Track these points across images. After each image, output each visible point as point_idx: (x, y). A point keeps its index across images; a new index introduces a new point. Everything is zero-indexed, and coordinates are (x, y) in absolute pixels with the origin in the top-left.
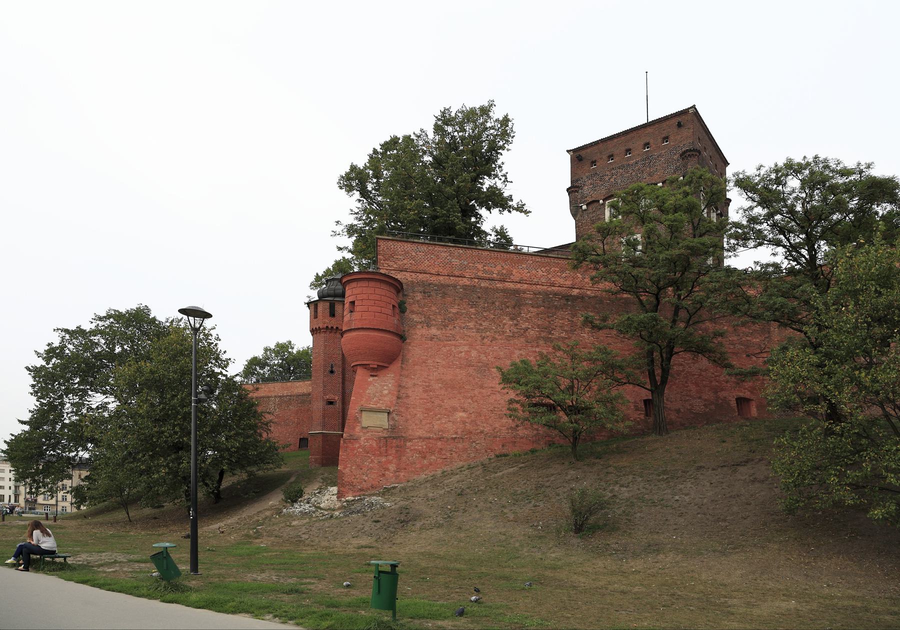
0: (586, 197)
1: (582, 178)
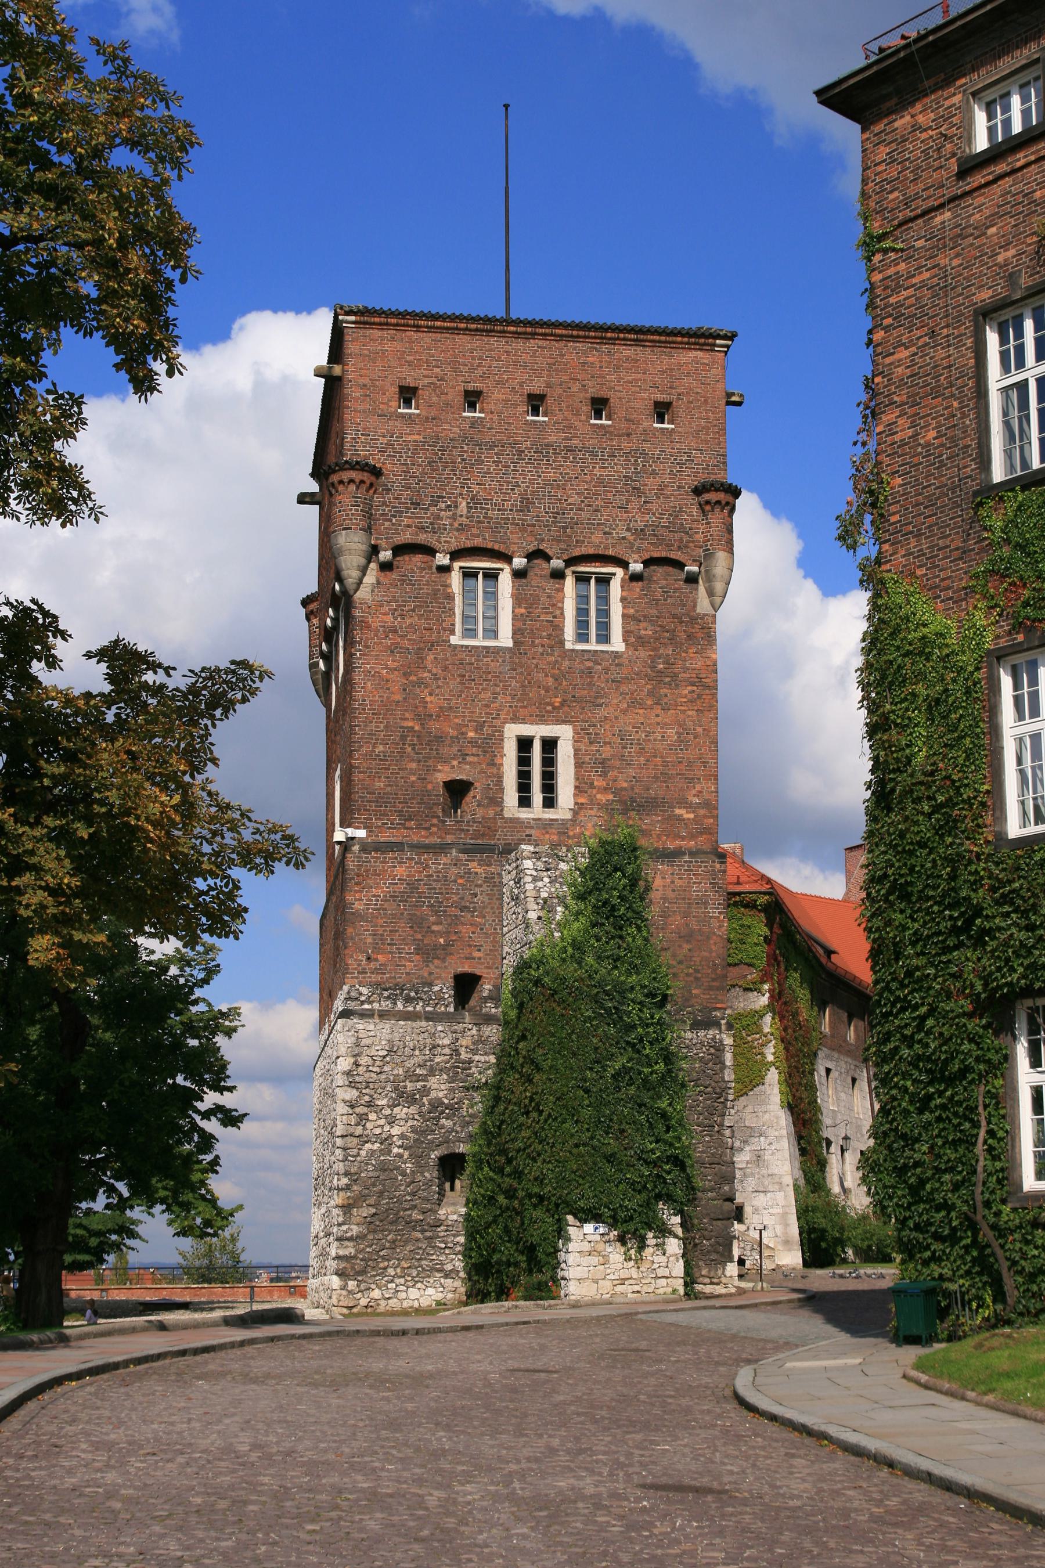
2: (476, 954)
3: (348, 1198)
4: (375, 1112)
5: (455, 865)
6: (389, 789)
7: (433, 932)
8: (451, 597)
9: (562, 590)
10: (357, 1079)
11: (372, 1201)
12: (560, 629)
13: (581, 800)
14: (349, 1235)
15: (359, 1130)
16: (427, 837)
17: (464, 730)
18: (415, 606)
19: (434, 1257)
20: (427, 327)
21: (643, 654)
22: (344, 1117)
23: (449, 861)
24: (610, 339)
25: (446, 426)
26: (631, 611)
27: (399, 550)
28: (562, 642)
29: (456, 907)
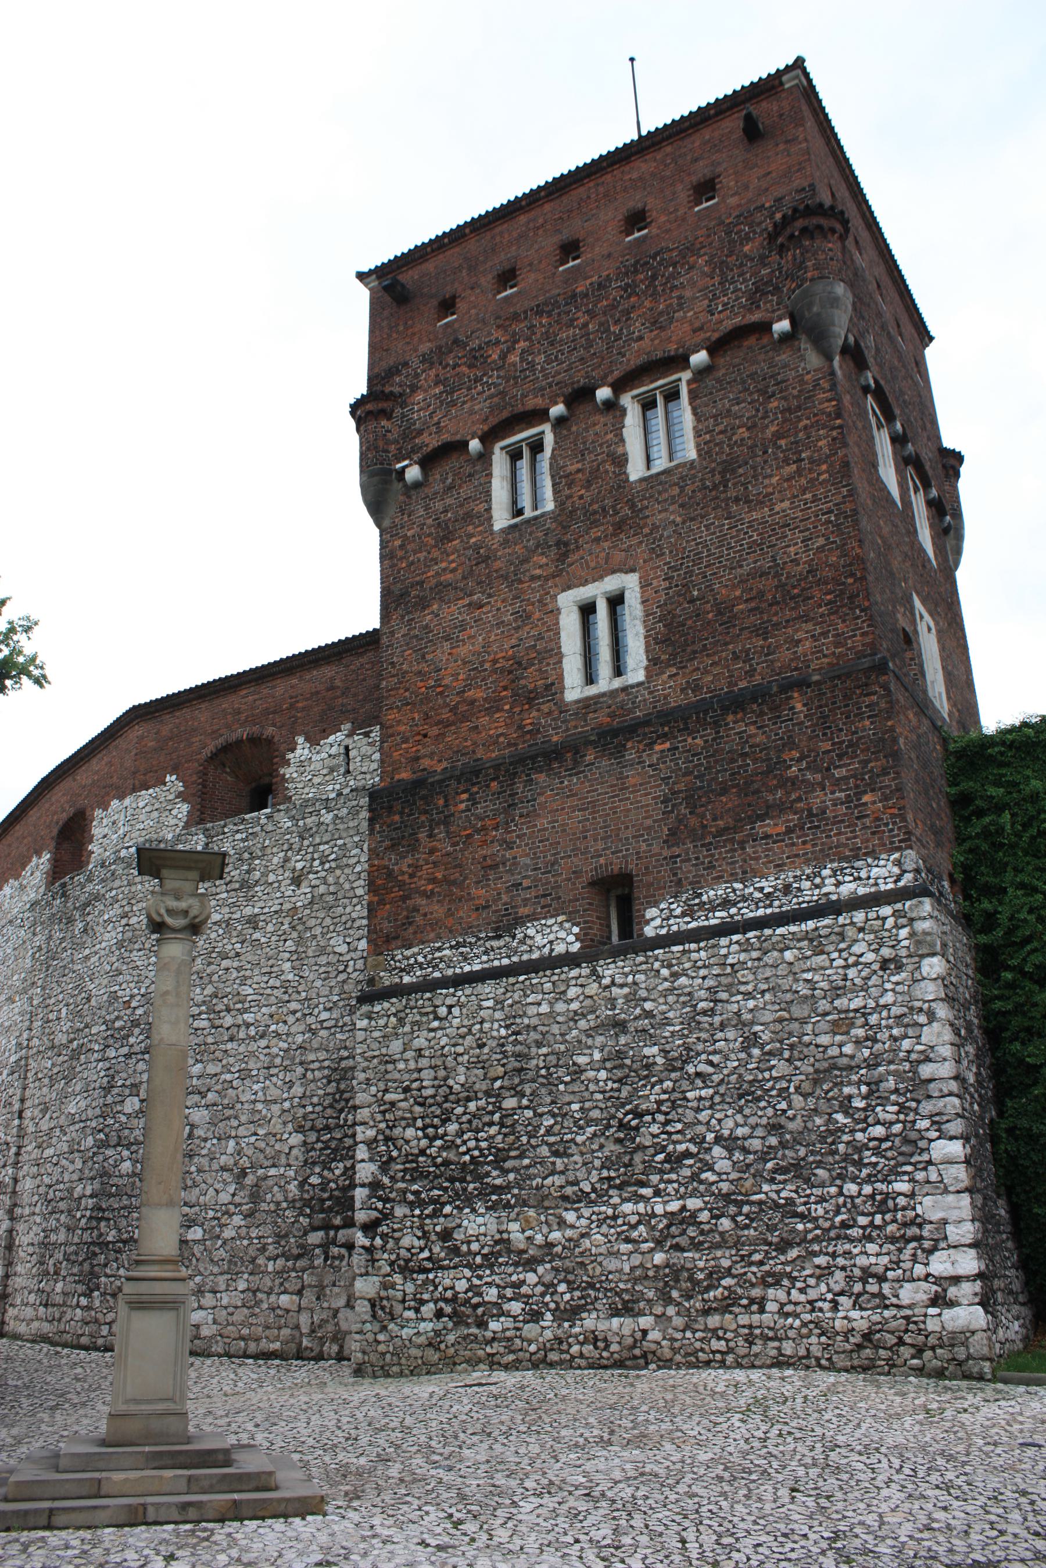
0: (420, 432)
1: (406, 364)
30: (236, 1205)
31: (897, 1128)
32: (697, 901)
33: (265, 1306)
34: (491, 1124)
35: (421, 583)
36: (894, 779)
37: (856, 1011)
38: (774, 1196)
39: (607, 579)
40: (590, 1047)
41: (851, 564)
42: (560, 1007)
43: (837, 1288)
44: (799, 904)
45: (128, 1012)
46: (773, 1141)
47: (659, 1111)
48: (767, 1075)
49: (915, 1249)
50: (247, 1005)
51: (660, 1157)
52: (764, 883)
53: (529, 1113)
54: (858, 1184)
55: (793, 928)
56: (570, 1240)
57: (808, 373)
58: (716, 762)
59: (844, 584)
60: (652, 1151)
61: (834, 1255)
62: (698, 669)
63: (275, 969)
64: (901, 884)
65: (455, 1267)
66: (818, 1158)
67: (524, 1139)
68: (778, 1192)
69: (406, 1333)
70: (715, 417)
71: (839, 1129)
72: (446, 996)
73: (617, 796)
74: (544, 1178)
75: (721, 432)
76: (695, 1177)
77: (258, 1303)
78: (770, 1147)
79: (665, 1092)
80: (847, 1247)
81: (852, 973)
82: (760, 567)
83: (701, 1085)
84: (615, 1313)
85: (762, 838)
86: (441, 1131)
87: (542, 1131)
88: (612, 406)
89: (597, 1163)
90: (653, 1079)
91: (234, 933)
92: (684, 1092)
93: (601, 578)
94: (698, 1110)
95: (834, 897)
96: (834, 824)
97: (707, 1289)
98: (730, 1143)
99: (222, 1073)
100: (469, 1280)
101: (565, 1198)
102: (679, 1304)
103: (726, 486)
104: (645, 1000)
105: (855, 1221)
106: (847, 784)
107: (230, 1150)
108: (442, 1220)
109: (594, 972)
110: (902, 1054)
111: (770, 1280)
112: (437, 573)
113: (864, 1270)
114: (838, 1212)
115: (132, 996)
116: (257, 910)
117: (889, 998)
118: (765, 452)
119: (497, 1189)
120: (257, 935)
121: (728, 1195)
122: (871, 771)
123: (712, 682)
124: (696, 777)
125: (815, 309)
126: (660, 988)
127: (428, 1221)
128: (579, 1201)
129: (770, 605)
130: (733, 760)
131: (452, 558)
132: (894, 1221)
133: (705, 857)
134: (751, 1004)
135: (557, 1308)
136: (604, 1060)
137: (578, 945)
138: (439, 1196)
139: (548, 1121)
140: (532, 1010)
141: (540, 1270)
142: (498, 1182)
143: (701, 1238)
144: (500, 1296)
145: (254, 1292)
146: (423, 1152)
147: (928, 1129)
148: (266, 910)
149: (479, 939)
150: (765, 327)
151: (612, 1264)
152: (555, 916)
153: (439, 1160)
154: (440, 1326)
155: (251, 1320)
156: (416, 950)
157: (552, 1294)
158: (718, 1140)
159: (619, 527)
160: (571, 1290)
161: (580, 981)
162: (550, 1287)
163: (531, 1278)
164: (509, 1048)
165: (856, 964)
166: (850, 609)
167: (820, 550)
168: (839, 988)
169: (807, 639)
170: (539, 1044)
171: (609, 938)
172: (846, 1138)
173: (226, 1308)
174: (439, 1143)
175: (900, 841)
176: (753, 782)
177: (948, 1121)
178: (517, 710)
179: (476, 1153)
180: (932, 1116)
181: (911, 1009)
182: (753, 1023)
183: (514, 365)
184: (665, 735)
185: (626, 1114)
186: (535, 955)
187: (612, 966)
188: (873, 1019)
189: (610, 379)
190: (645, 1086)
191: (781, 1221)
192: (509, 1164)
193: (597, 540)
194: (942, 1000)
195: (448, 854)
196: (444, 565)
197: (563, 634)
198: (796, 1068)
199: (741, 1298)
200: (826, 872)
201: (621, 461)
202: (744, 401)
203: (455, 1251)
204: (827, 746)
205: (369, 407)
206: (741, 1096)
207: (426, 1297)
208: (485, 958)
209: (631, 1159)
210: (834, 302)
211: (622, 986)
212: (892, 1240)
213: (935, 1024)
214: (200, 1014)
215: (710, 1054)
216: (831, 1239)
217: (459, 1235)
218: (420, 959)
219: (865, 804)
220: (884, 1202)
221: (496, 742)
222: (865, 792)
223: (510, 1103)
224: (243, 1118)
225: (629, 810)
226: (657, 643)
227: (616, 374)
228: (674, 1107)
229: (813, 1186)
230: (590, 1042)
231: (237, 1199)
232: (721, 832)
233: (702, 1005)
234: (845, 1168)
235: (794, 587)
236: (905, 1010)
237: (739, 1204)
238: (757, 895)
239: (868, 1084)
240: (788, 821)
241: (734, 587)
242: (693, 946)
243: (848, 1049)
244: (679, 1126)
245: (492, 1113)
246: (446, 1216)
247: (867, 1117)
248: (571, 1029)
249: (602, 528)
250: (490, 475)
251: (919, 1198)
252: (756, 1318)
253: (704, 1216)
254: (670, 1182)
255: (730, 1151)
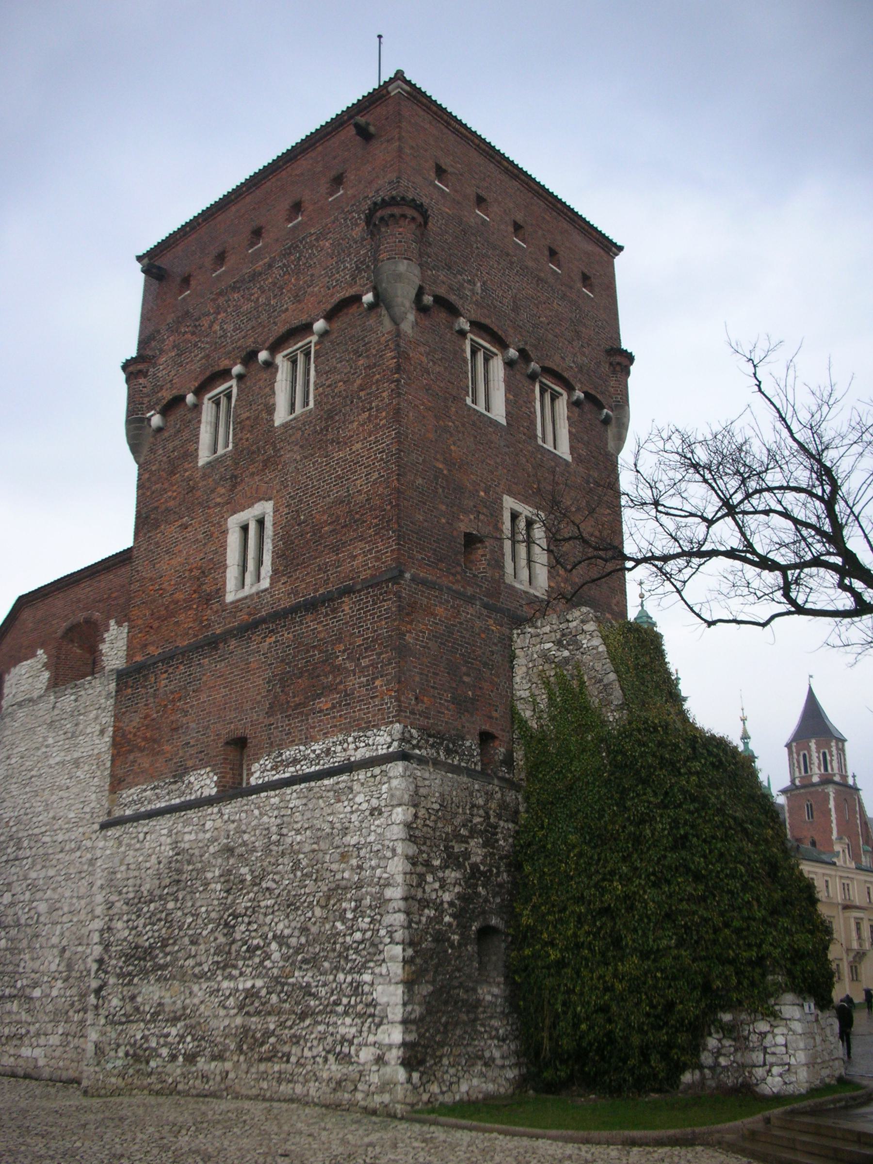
2: (494, 714)
3: (414, 972)
4: (432, 873)
5: (479, 618)
6: (426, 524)
7: (464, 682)
8: (465, 360)
9: (533, 391)
10: (417, 833)
11: (430, 976)
12: (533, 423)
13: (552, 584)
14: (413, 1016)
15: (419, 895)
16: (453, 583)
17: (477, 487)
18: (442, 358)
19: (476, 1043)
20: (454, 128)
21: (581, 469)
22: (408, 876)
23: (474, 613)
24: (558, 209)
25: (466, 213)
26: (574, 430)
27: (439, 301)
28: (536, 436)
29: (480, 661)
30: (61, 973)
31: (369, 934)
32: (280, 759)
33: (72, 1046)
34: (160, 920)
35: (157, 508)
36: (394, 668)
37: (354, 846)
38: (300, 979)
39: (256, 506)
40: (214, 866)
41: (389, 495)
42: (201, 836)
43: (328, 1048)
44: (334, 763)
45: (8, 829)
46: (303, 940)
47: (245, 915)
48: (303, 891)
49: (371, 1023)
50: (71, 826)
51: (245, 948)
52: (316, 747)
53: (179, 913)
54: (346, 974)
55: (326, 782)
56: (194, 1005)
57: (383, 335)
58: (298, 652)
59: (385, 510)
60: (240, 943)
61: (328, 1024)
62: (298, 578)
63: (87, 799)
64: (391, 750)
65: (136, 1022)
66: (325, 954)
67: (176, 932)
68: (303, 977)
69: (109, 1066)
70: (326, 373)
71: (338, 934)
72: (144, 826)
73: (244, 677)
74: (185, 960)
75: (329, 386)
76: (262, 962)
77: (68, 1043)
78: (301, 944)
79: (250, 900)
80: (335, 1019)
81: (354, 817)
82: (340, 496)
83: (268, 897)
84: (214, 1058)
85: (319, 712)
86: (135, 924)
87: (186, 927)
88: (270, 365)
89: (212, 951)
90: (245, 891)
91: (66, 772)
92: (259, 902)
93: (253, 504)
94: (266, 915)
95: (352, 759)
96: (358, 702)
97: (262, 1044)
98: (281, 940)
99: (56, 876)
100: (143, 1031)
101: (195, 975)
102: (246, 1054)
103: (327, 430)
104: (245, 832)
105: (341, 1000)
106: (368, 671)
107: (57, 933)
108: (132, 987)
109: (220, 811)
110: (376, 880)
111: (294, 1040)
112: (166, 501)
113: (343, 1037)
114: (332, 994)
115: (11, 818)
116: (80, 754)
117: (372, 838)
118: (352, 402)
119: (163, 967)
120: (78, 774)
121: (277, 978)
122: (382, 662)
123: (305, 588)
124: (287, 664)
125: (384, 285)
126: (253, 824)
127: (125, 988)
128: (201, 978)
129: (343, 527)
130: (308, 651)
131: (175, 488)
132: (361, 1002)
133: (287, 725)
134: (299, 838)
135: (185, 1053)
136: (221, 876)
137: (215, 790)
138: (133, 971)
139: (189, 920)
140: (187, 837)
141: (179, 1025)
142: (162, 961)
143: (261, 1008)
144: (158, 1043)
145: (67, 1035)
146: (125, 939)
147: (384, 937)
148: (85, 754)
149: (166, 783)
150: (357, 299)
151: (214, 1023)
152: (206, 767)
153: (133, 945)
154: (126, 1063)
155: (65, 1056)
156: (132, 790)
157: (184, 1043)
158: (275, 937)
159: (266, 463)
160: (193, 1040)
161: (213, 817)
162: (182, 1037)
163: (174, 1031)
164: (173, 865)
165: (357, 810)
166: (387, 530)
167: (375, 482)
168: (347, 829)
169: (360, 554)
170: (189, 863)
171: (241, 784)
172: (341, 940)
173: (52, 1046)
174: (134, 932)
175: (393, 717)
176: (317, 668)
177: (396, 931)
178: (200, 608)
179: (152, 941)
180: (387, 927)
181: (383, 845)
182: (299, 852)
183: (215, 332)
184: (273, 631)
185: (229, 916)
186: (193, 797)
187: (229, 806)
188: (362, 852)
189: (267, 345)
190: (240, 895)
191: (303, 997)
192: (168, 949)
193: (253, 474)
194: (402, 839)
195: (153, 720)
196: (169, 494)
197: (228, 550)
198: (319, 887)
199: (278, 1052)
200: (350, 739)
201: (271, 410)
202: (344, 360)
203: (137, 1009)
204: (359, 641)
205: (131, 369)
206: (288, 906)
207: (121, 1041)
208: (167, 797)
209: (230, 949)
210: (399, 277)
211: (233, 822)
212: (359, 1015)
213: (396, 858)
214: (46, 832)
215: (275, 874)
216: (327, 1013)
217: (139, 999)
218: (135, 798)
219: (376, 687)
220: (357, 988)
221: (187, 634)
222: (377, 678)
223: (171, 905)
224: (66, 909)
225: (249, 689)
226: (278, 558)
227: (271, 340)
228: (254, 912)
229: (321, 974)
230: (214, 862)
231: (61, 968)
232: (297, 706)
233: (275, 838)
234: (339, 962)
235: (357, 513)
236: (380, 847)
237: (283, 985)
238: (312, 756)
239: (356, 901)
240: (334, 699)
241: (324, 512)
242: (272, 793)
243: (346, 875)
244: (255, 926)
245: (162, 912)
246: (135, 985)
247: (353, 925)
248: (206, 852)
249: (256, 465)
250: (199, 422)
251: (375, 986)
252: (283, 1066)
253: (263, 992)
254: (248, 966)
255: (281, 946)
